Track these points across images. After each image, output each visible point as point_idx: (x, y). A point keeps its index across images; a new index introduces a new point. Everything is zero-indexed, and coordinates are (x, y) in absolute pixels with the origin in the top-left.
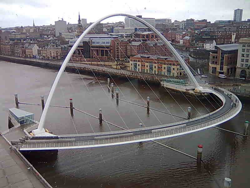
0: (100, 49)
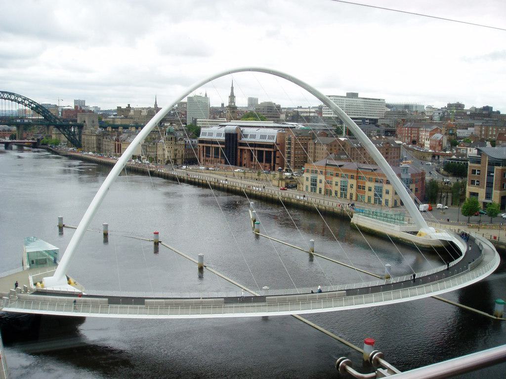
0: (256, 149)
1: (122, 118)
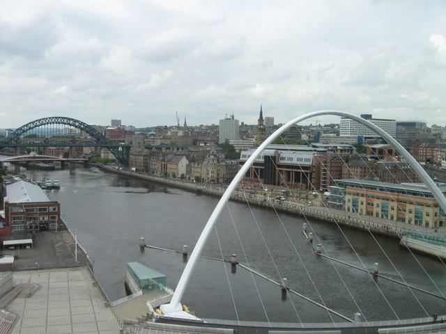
0: (294, 170)
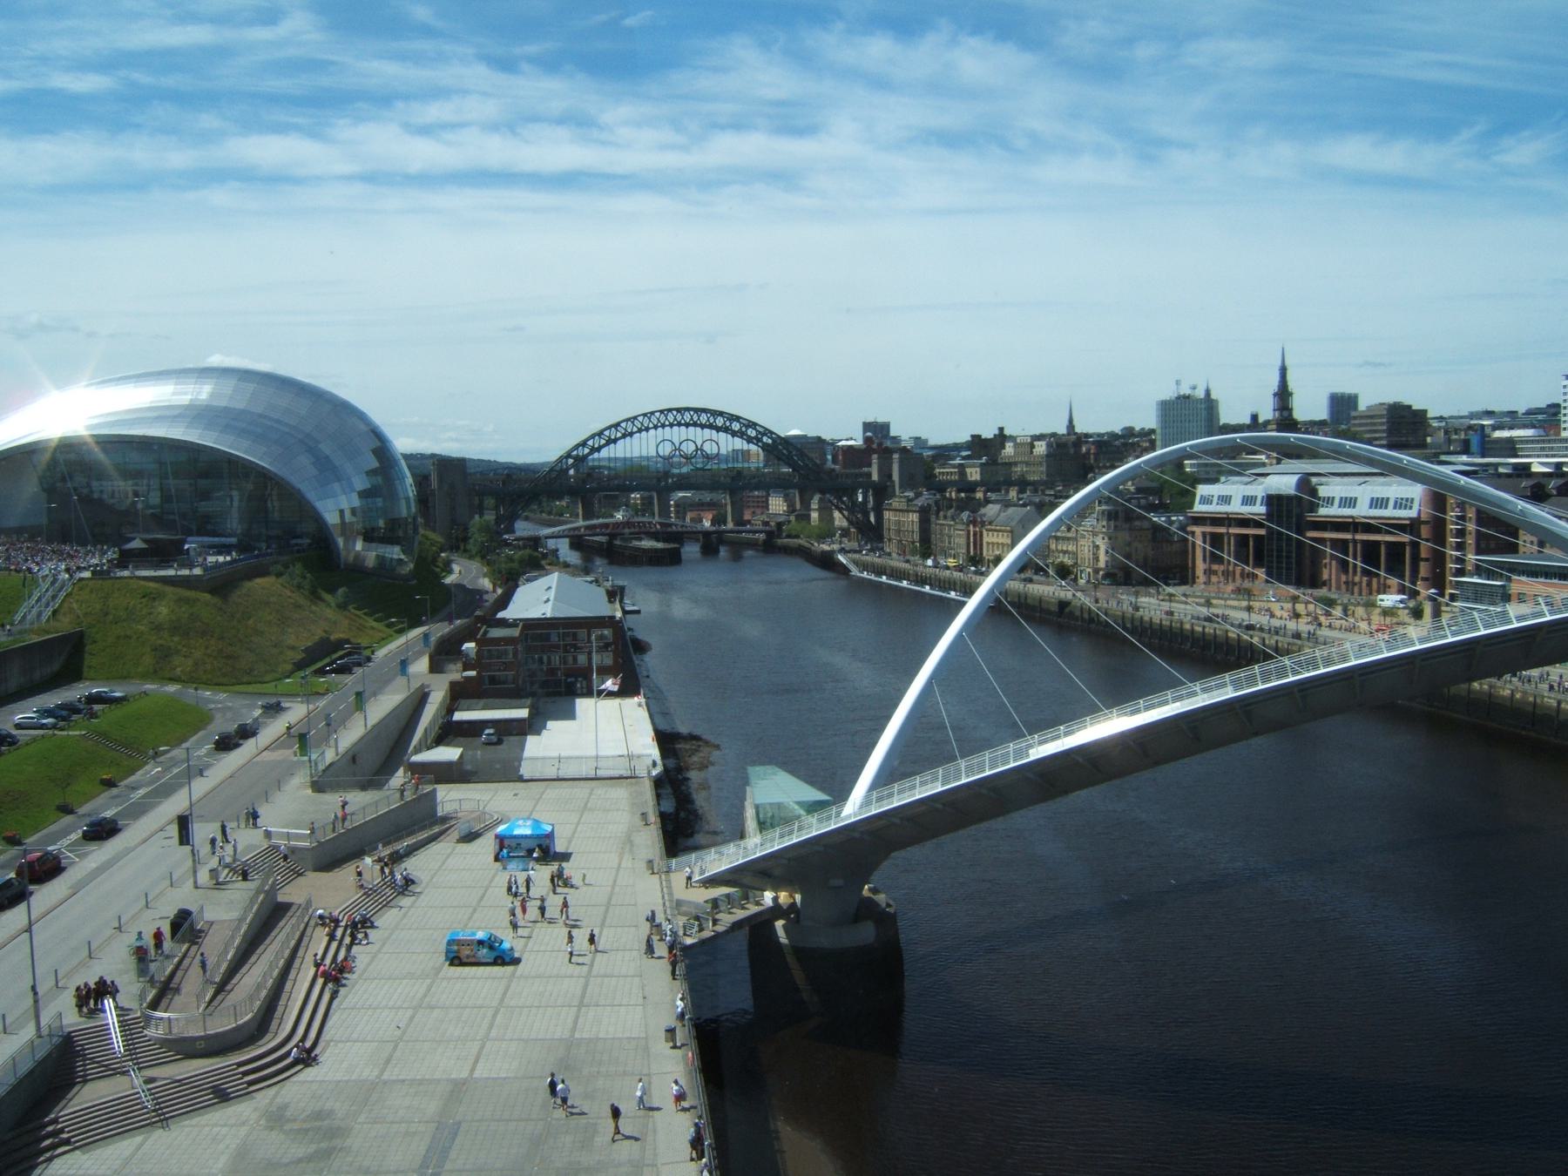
0: (1359, 537)
1: (982, 465)
